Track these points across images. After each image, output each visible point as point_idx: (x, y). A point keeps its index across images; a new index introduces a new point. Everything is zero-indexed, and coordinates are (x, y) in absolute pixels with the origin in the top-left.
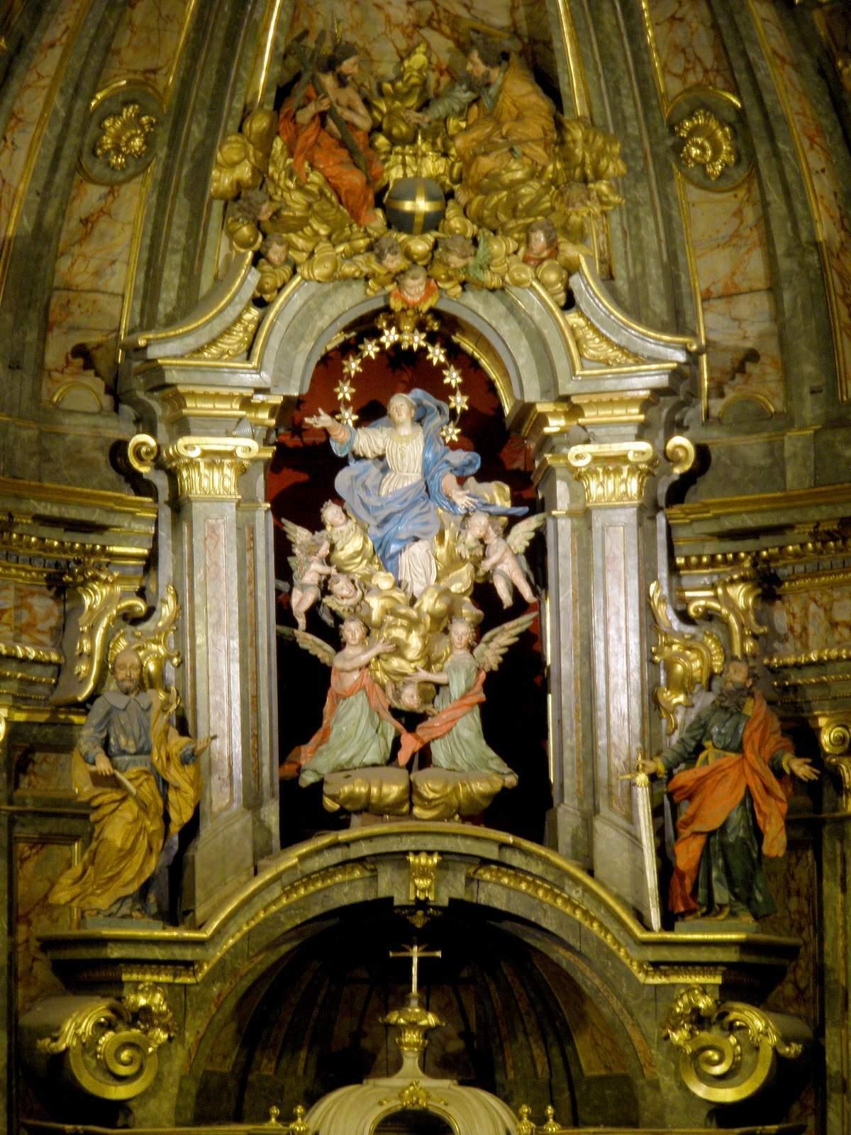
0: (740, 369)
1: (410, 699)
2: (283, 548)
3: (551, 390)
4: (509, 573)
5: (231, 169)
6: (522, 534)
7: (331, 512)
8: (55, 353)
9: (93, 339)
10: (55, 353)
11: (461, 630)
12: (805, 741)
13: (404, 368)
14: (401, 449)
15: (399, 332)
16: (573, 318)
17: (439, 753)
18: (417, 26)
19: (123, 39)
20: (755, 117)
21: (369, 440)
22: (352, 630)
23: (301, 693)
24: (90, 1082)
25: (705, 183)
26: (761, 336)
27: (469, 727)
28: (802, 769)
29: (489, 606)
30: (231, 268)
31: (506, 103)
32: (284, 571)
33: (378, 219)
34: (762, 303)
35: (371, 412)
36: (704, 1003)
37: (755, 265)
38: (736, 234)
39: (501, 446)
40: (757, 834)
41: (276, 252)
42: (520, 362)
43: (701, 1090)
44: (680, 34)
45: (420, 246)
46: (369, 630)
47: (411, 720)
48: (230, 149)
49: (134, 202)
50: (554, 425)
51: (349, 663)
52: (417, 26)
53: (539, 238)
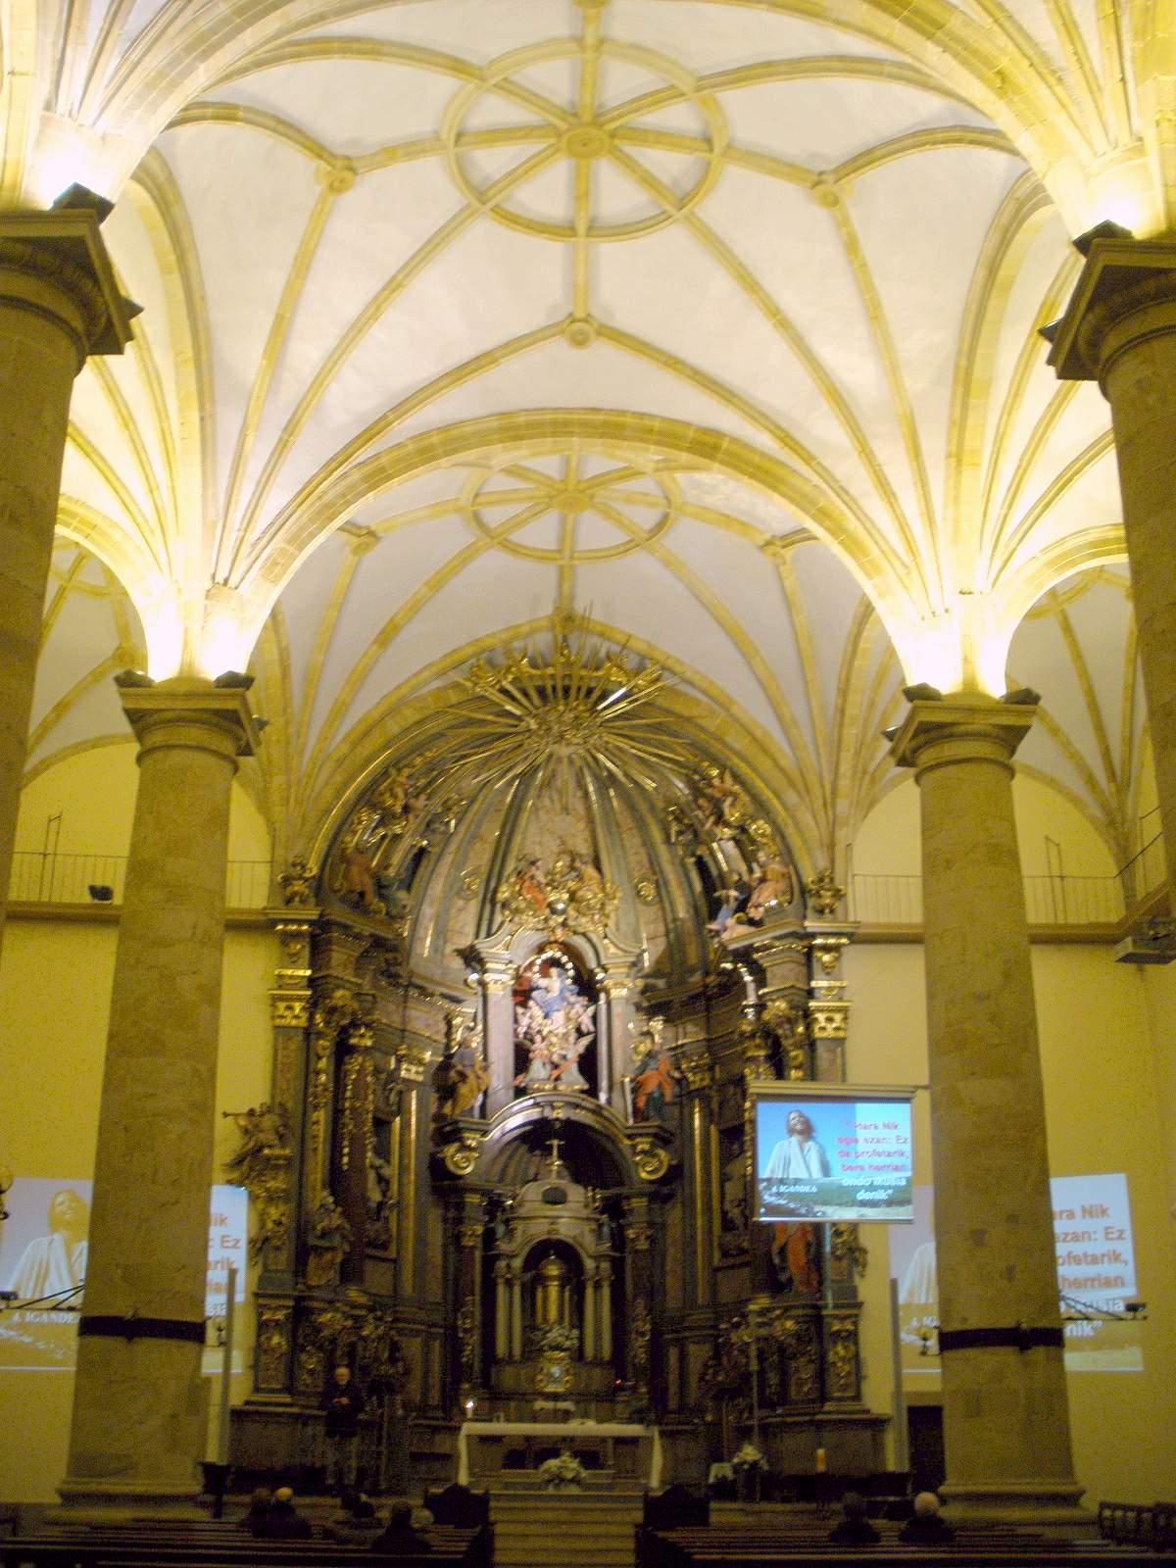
1: (555, 1058)
3: (599, 965)
4: (586, 1024)
5: (504, 893)
6: (591, 1009)
7: (531, 1003)
8: (449, 949)
10: (449, 949)
11: (572, 1039)
12: (678, 1068)
13: (554, 963)
14: (556, 984)
16: (606, 941)
17: (563, 1076)
19: (471, 854)
20: (661, 882)
21: (543, 982)
22: (538, 1038)
23: (522, 1058)
24: (451, 1168)
25: (647, 904)
27: (574, 1068)
28: (677, 1075)
29: (580, 1033)
30: (502, 924)
31: (586, 877)
32: (516, 1021)
33: (547, 911)
35: (545, 973)
36: (647, 1147)
37: (662, 929)
39: (587, 987)
40: (662, 1095)
41: (516, 919)
43: (644, 1175)
46: (543, 1039)
47: (556, 1066)
48: (504, 888)
49: (474, 906)
50: (599, 977)
51: (539, 1047)
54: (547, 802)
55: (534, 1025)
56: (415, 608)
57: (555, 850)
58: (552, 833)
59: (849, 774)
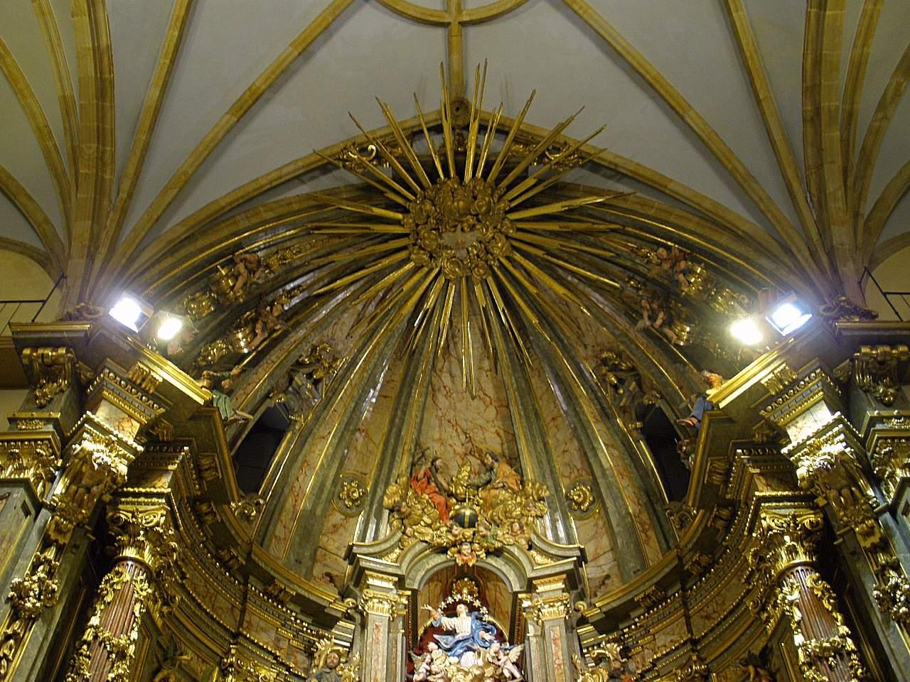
0: (603, 583)
2: (410, 660)
6: (515, 652)
9: (334, 573)
15: (461, 595)
18: (466, 454)
25: (583, 515)
26: (610, 569)
34: (610, 555)
37: (605, 542)
38: (596, 533)
42: (510, 579)
44: (567, 458)
45: (469, 532)
48: (393, 488)
52: (466, 454)
53: (516, 526)
54: (446, 380)
55: (434, 668)
56: (281, 76)
57: (460, 450)
58: (455, 425)
59: (840, 193)
